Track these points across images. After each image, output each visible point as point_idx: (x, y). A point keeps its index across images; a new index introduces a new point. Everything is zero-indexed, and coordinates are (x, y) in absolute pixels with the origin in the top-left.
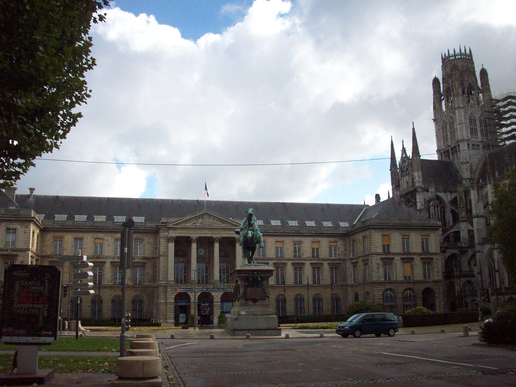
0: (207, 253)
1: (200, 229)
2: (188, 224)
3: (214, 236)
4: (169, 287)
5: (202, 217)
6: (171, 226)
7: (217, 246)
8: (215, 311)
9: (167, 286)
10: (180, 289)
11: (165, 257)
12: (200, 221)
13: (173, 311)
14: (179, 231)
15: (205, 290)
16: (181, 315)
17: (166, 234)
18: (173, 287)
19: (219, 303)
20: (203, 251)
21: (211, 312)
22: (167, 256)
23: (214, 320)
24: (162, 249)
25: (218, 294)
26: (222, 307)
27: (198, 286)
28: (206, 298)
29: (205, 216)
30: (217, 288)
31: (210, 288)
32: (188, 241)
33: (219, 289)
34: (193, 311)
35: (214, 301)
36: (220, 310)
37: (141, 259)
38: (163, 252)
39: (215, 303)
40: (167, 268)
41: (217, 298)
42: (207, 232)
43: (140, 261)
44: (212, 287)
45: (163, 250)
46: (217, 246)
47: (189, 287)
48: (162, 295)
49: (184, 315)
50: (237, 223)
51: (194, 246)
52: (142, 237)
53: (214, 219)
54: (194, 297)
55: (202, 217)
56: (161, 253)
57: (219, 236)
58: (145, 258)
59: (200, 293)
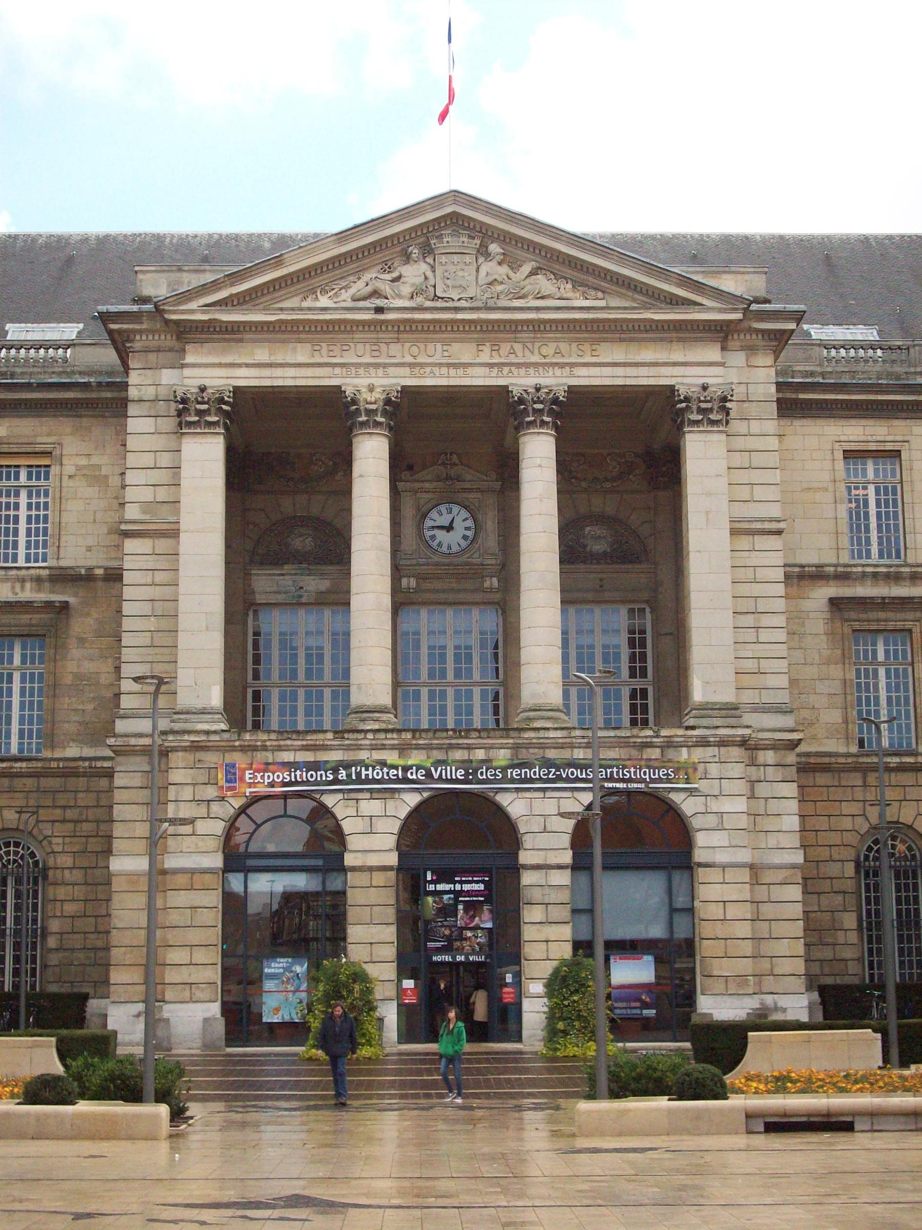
0: (491, 541)
1: (407, 329)
2: (324, 301)
3: (520, 382)
4: (177, 759)
5: (427, 251)
6: (195, 311)
7: (538, 454)
8: (528, 933)
9: (165, 753)
10: (266, 767)
11: (163, 545)
12: (414, 273)
13: (215, 935)
14: (262, 354)
15: (451, 777)
16: (275, 966)
17: (168, 377)
18: (212, 758)
19: (563, 878)
20: (462, 520)
21: (506, 945)
22: (174, 534)
23: (526, 1004)
24: (140, 491)
25: (548, 805)
26: (584, 911)
27: (403, 749)
28: (460, 837)
29: (450, 241)
30: (548, 764)
31: (487, 761)
32: (327, 418)
33: (558, 773)
34: (372, 942)
35: (525, 857)
36: (566, 932)
37: (38, 580)
38: (147, 506)
39: (527, 878)
40: (168, 615)
41: (543, 841)
42: (463, 352)
43: (28, 594)
44: (502, 757)
45: (147, 495)
46: (538, 454)
47: (335, 756)
48: (130, 815)
49: (300, 969)
50: (685, 282)
51: (371, 456)
52: (44, 440)
53: (515, 266)
54: (373, 833)
55: (427, 251)
56: (132, 512)
57: (557, 381)
58: (63, 577)
59: (413, 800)
